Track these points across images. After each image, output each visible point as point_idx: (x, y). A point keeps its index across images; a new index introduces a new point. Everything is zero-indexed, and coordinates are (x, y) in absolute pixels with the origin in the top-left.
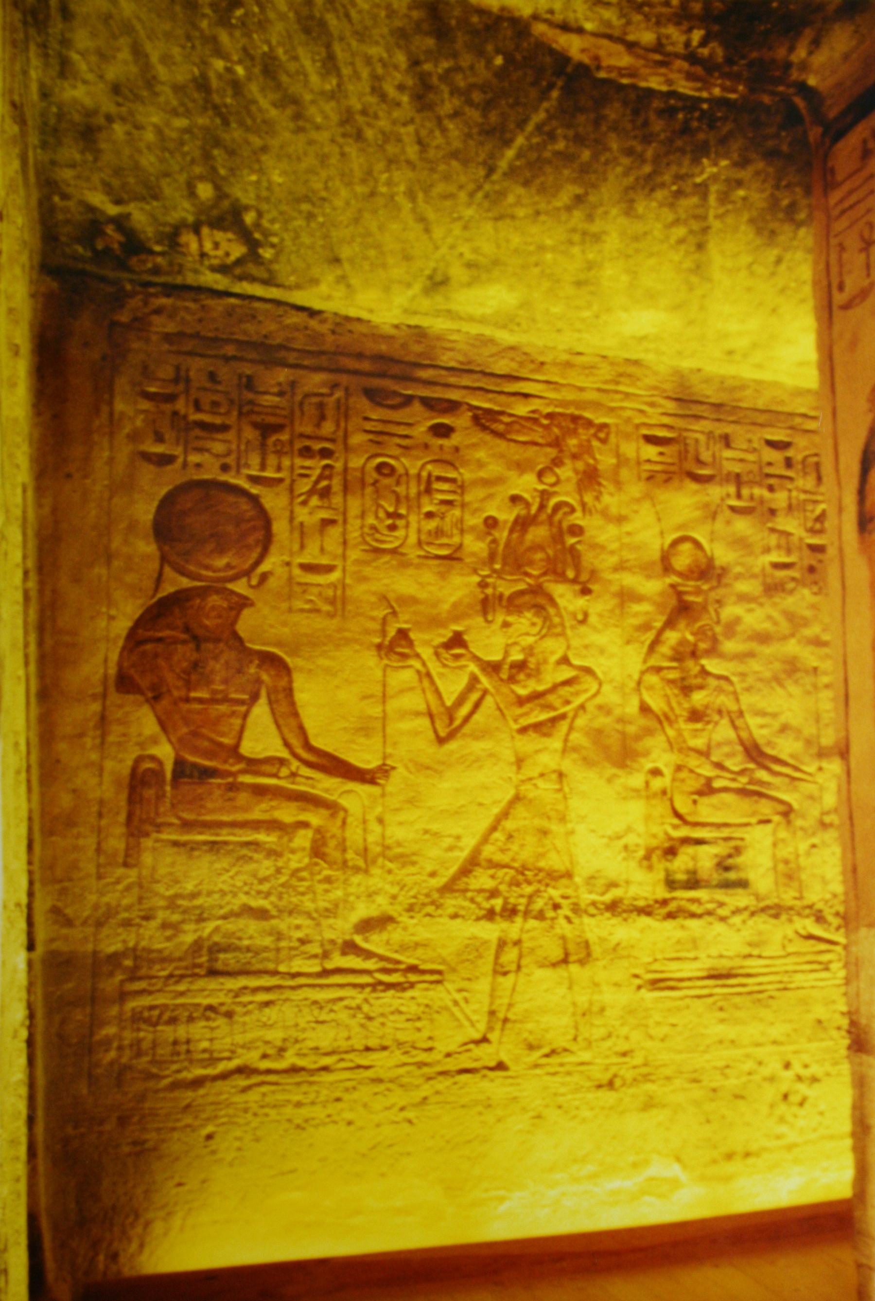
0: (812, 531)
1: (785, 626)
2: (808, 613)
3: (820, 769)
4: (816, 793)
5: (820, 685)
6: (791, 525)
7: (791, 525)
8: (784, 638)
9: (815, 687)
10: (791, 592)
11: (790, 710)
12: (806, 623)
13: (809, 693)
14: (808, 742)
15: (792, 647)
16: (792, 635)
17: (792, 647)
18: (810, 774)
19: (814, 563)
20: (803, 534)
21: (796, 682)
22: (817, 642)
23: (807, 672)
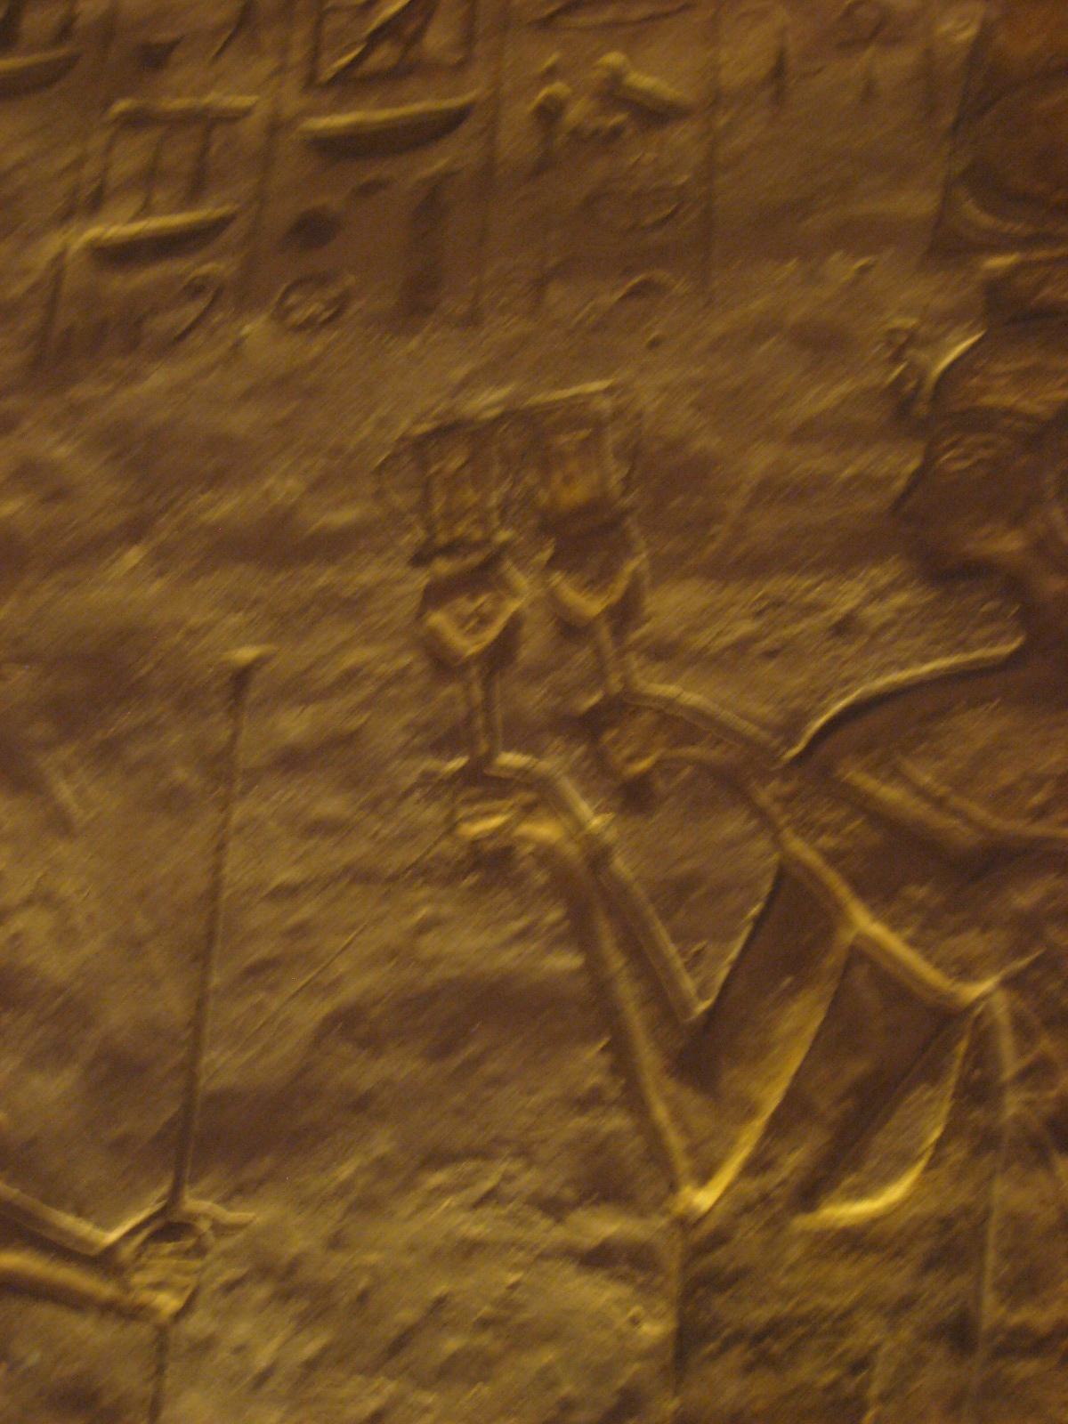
0: (350, 84)
1: (101, 491)
2: (241, 422)
3: (169, 1227)
4: (129, 1379)
5: (251, 754)
6: (244, 91)
7: (244, 91)
8: (98, 548)
9: (220, 767)
10: (173, 343)
11: (43, 899)
12: (228, 462)
13: (173, 801)
14: (118, 1072)
15: (124, 586)
16: (135, 531)
17: (124, 586)
18: (104, 1262)
19: (331, 200)
20: (293, 102)
21: (108, 753)
22: (276, 544)
23: (187, 700)
